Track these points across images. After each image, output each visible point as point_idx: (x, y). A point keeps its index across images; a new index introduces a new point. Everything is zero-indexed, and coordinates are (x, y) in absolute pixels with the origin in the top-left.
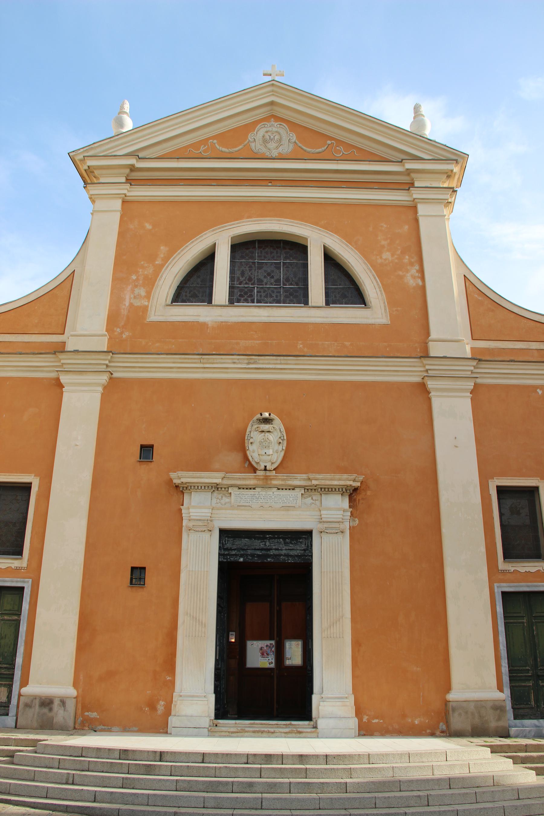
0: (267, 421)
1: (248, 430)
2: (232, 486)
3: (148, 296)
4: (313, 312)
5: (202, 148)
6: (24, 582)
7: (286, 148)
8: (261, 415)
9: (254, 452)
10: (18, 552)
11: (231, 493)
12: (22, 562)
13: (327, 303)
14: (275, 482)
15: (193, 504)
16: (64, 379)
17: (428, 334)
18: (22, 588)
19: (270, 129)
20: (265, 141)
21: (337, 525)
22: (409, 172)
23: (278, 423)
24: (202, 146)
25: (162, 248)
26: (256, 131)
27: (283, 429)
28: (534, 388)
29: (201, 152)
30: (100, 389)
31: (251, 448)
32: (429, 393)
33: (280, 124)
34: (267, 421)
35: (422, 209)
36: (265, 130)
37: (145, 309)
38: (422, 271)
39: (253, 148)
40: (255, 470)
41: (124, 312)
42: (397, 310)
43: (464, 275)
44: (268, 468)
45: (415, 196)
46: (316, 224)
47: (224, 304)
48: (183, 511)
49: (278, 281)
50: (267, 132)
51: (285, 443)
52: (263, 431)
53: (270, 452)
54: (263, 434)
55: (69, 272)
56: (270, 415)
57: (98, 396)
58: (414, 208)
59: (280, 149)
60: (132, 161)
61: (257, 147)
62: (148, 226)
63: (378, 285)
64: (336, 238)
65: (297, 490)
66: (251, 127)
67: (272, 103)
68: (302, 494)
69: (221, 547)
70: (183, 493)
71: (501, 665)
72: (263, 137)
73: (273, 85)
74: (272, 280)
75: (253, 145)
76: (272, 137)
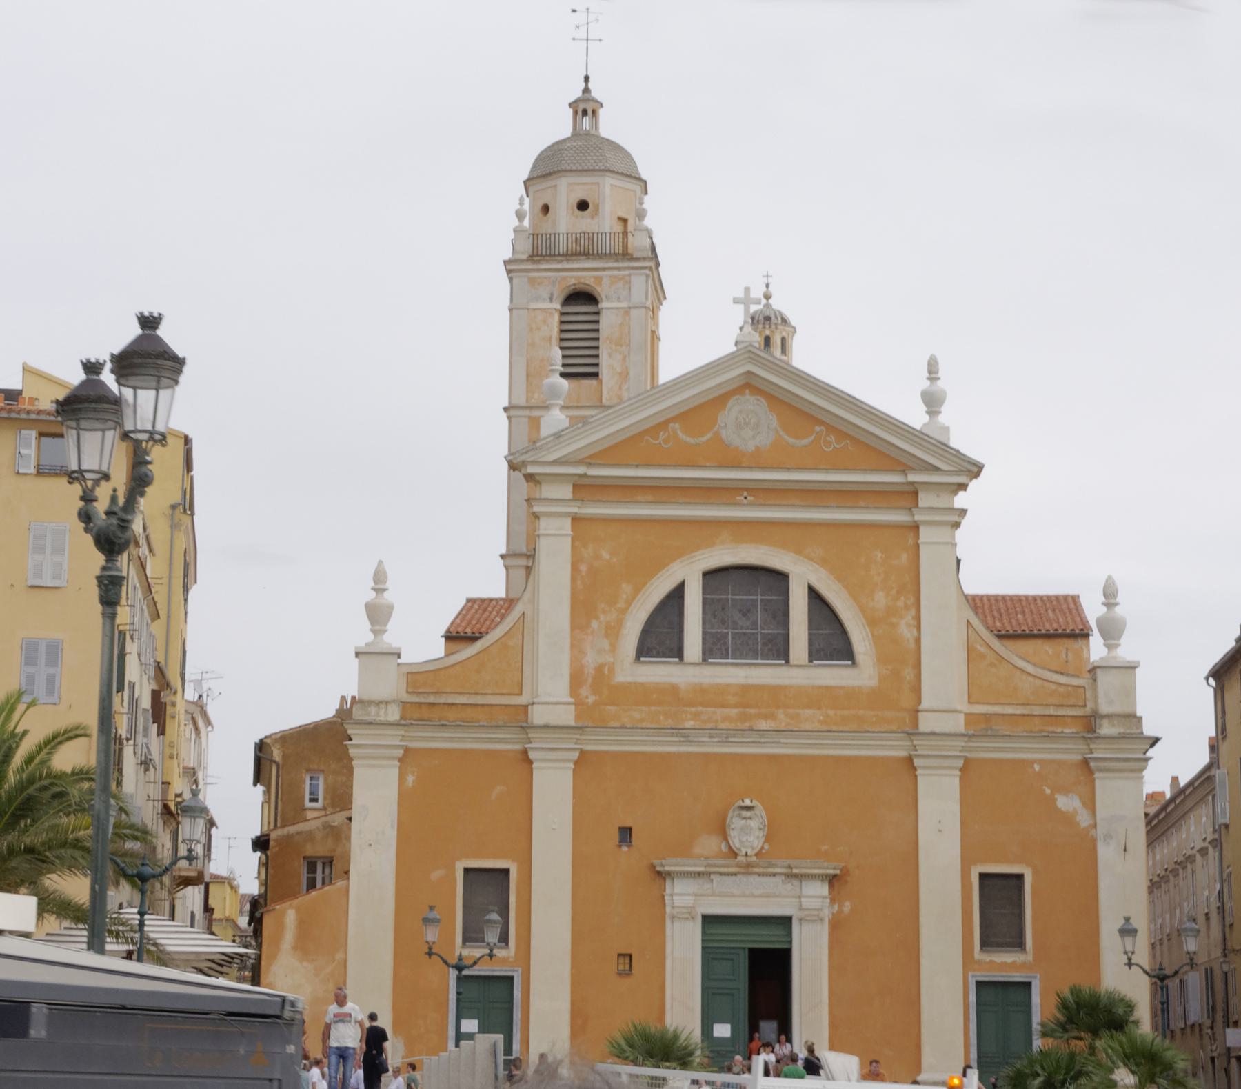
0: (748, 808)
1: (730, 815)
2: (714, 873)
3: (613, 648)
4: (794, 672)
5: (662, 436)
6: (513, 971)
8: (743, 801)
9: (734, 837)
11: (712, 880)
13: (810, 661)
14: (756, 870)
15: (676, 891)
16: (532, 755)
17: (919, 702)
18: (511, 978)
21: (816, 913)
22: (912, 483)
23: (760, 810)
24: (662, 433)
25: (624, 585)
26: (727, 409)
27: (764, 814)
28: (1033, 762)
29: (660, 443)
30: (572, 766)
31: (732, 833)
32: (915, 769)
33: (758, 400)
34: (748, 808)
35: (925, 534)
37: (611, 670)
38: (918, 618)
40: (735, 855)
41: (590, 670)
42: (888, 670)
43: (968, 621)
44: (749, 854)
45: (917, 518)
46: (798, 552)
47: (697, 662)
48: (666, 898)
49: (755, 624)
50: (740, 412)
51: (766, 829)
52: (744, 818)
53: (751, 839)
54: (744, 821)
56: (751, 801)
57: (570, 773)
58: (917, 527)
60: (581, 470)
62: (606, 555)
63: (868, 636)
64: (823, 573)
65: (777, 877)
66: (720, 401)
67: (749, 373)
68: (782, 881)
69: (704, 933)
70: (664, 879)
71: (970, 1052)
72: (737, 419)
73: (751, 348)
74: (749, 623)
75: (724, 433)
76: (747, 420)
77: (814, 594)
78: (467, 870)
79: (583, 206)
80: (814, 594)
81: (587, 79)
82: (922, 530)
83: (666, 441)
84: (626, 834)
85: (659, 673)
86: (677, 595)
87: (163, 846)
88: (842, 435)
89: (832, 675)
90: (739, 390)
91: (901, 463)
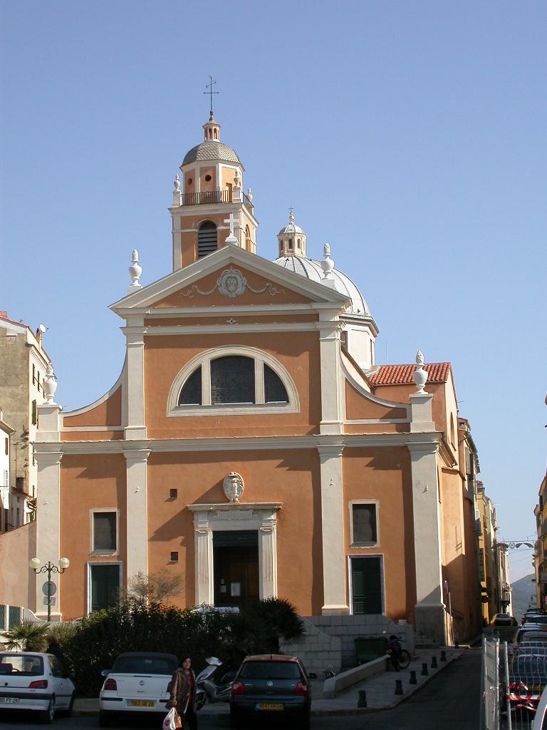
5: (189, 292)
7: (241, 290)
10: (113, 547)
12: (116, 554)
13: (266, 402)
19: (230, 275)
20: (227, 286)
36: (226, 277)
39: (220, 291)
45: (318, 327)
50: (228, 278)
55: (118, 386)
59: (237, 291)
61: (223, 290)
67: (231, 257)
75: (220, 289)
77: (267, 369)
78: (97, 515)
79: (208, 178)
80: (267, 369)
81: (211, 113)
82: (321, 333)
83: (191, 295)
84: (174, 493)
85: (191, 412)
86: (198, 372)
87: (18, 509)
88: (279, 287)
89: (276, 409)
90: (228, 267)
91: (306, 300)
